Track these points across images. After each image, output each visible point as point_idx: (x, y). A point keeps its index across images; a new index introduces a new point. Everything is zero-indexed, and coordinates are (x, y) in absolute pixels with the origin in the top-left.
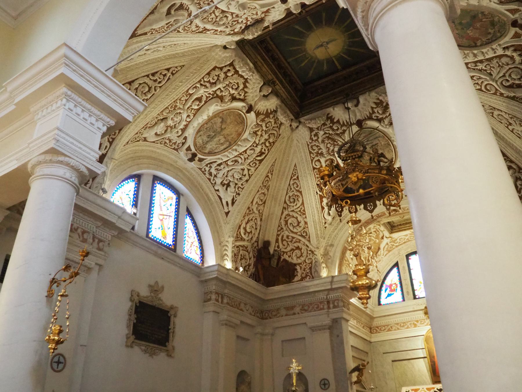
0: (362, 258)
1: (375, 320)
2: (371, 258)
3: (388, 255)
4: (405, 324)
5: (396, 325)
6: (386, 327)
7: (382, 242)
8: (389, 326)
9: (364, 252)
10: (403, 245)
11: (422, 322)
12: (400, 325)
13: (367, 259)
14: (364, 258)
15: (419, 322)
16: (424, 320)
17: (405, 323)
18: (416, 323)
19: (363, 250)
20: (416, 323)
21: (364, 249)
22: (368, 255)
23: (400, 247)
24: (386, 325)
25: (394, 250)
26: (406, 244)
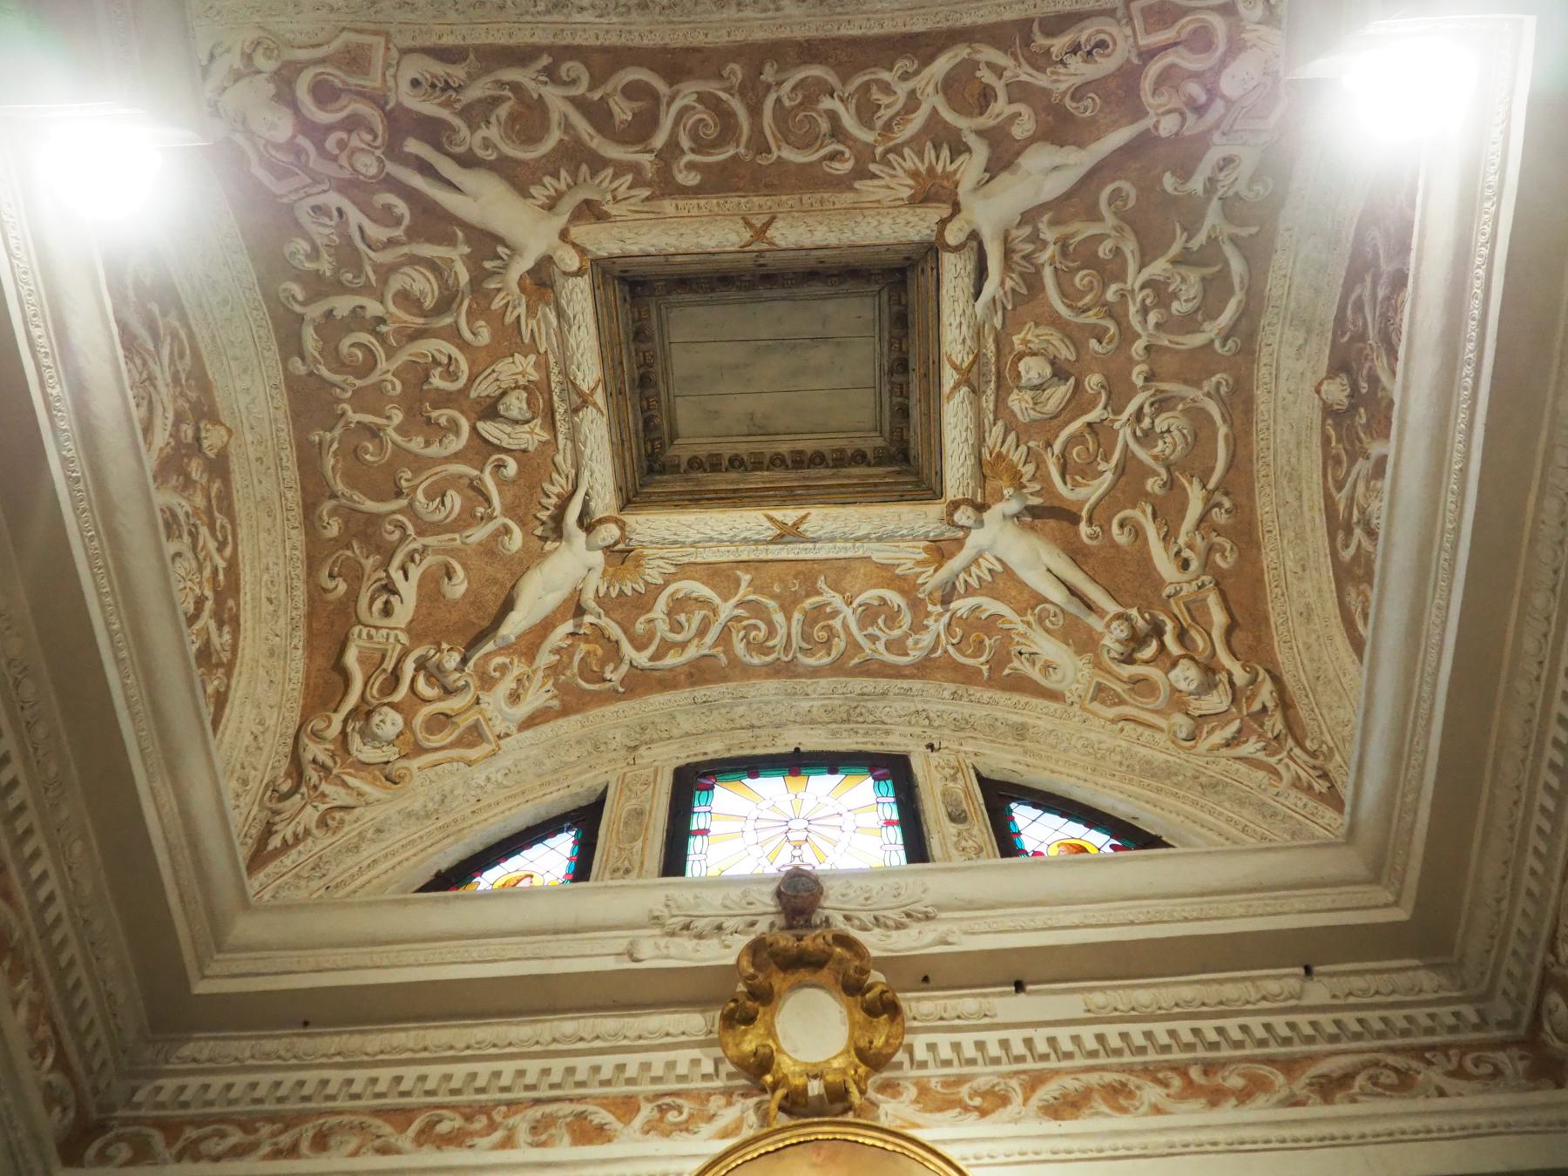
0: (351, 658)
1: (201, 1048)
2: (421, 665)
3: (546, 730)
4: (481, 1122)
5: (377, 1122)
6: (265, 1130)
7: (543, 556)
8: (308, 1130)
9: (387, 611)
10: (683, 696)
11: (672, 1116)
12: (431, 1125)
13: (389, 665)
14: (361, 660)
15: (647, 1111)
16: (703, 1097)
17: (485, 1109)
18: (602, 1116)
19: (390, 589)
20: (602, 1116)
21: (397, 576)
22: (404, 638)
23: (658, 701)
24: (271, 1118)
25: (609, 709)
26: (701, 692)
